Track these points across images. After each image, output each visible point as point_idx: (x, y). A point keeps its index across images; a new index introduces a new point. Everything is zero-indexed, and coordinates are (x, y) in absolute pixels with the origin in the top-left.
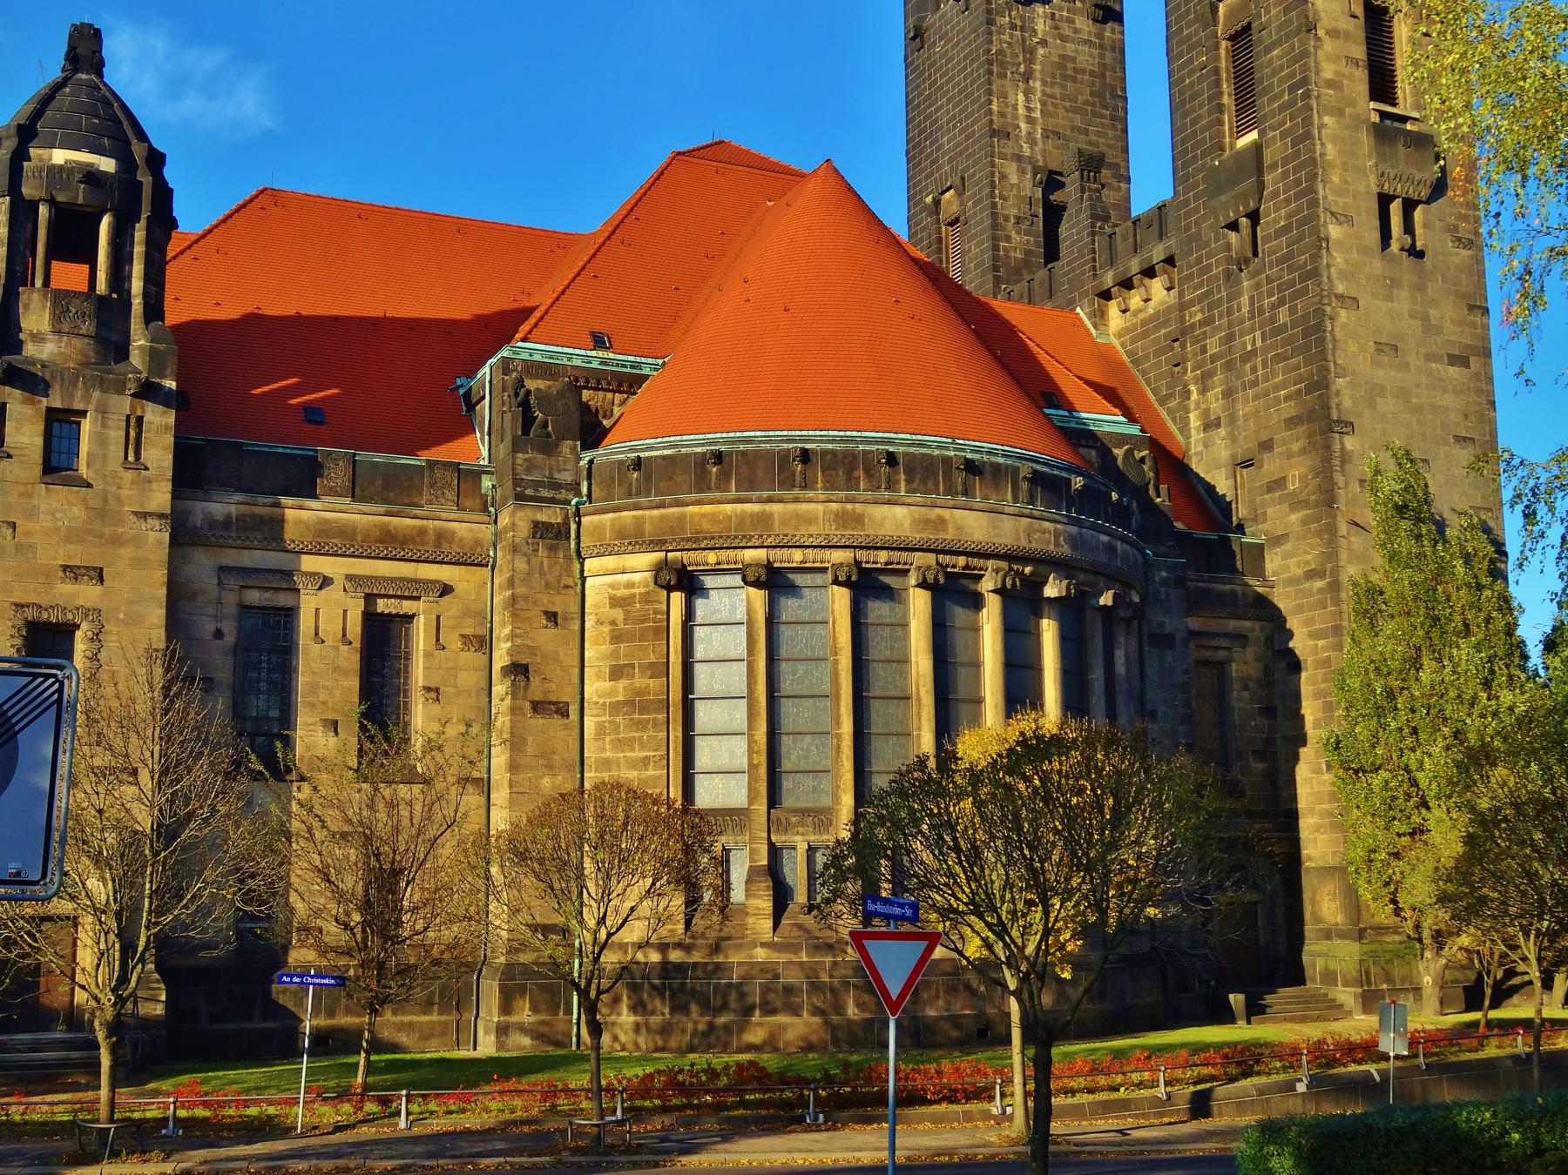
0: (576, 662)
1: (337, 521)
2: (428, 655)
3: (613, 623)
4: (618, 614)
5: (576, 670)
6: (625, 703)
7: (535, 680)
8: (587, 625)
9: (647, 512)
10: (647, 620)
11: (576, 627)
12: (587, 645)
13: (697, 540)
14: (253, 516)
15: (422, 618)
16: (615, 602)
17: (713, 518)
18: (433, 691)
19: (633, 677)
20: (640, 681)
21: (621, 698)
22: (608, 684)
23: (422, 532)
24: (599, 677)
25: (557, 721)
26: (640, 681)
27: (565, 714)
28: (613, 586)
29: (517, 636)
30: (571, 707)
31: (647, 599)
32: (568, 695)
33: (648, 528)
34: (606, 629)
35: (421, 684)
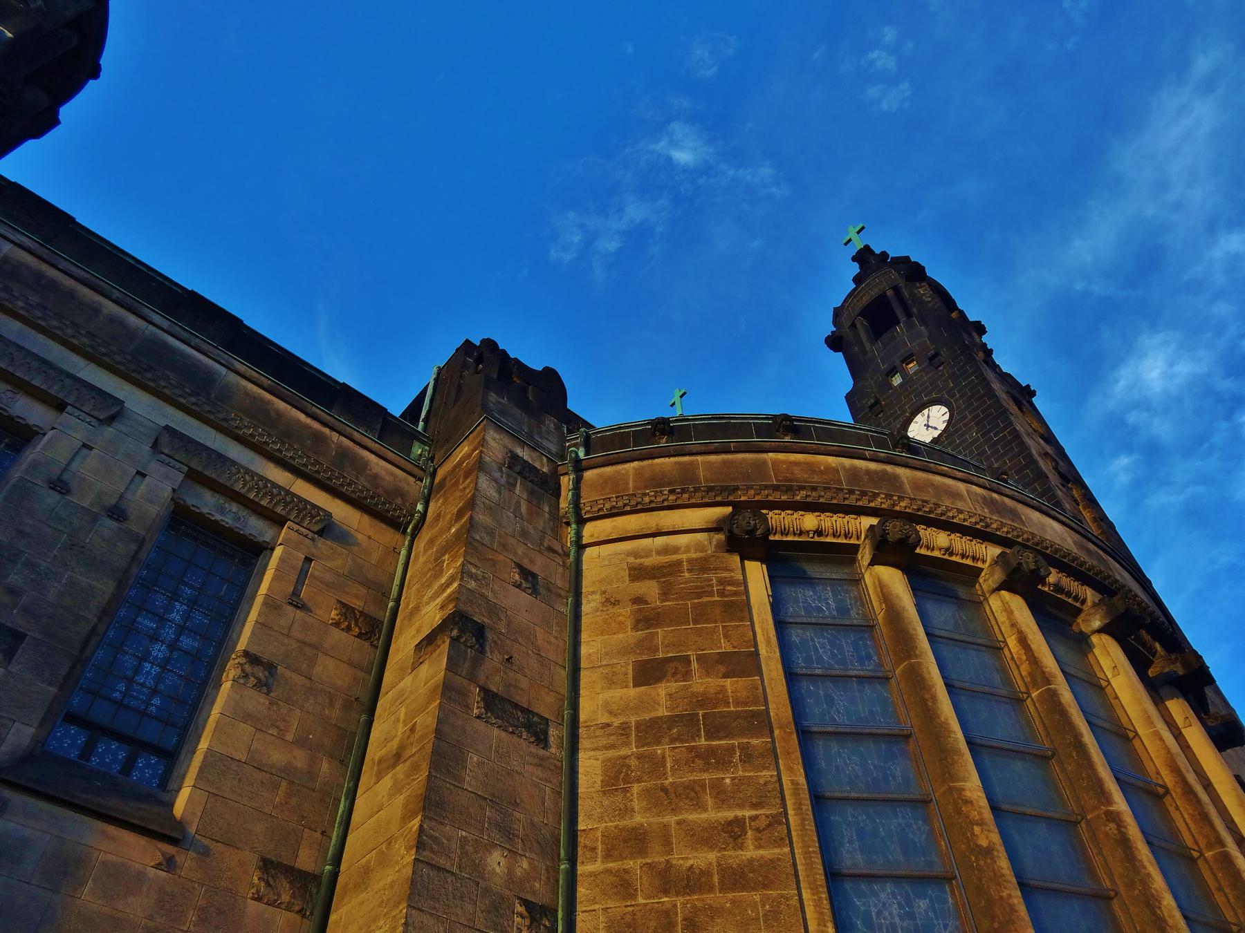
0: (566, 659)
1: (188, 356)
2: (270, 604)
3: (638, 600)
4: (650, 589)
5: (563, 675)
6: (673, 720)
7: (493, 659)
8: (586, 608)
9: (699, 458)
10: (711, 594)
11: (567, 610)
12: (584, 636)
13: (789, 489)
14: (39, 276)
15: (278, 551)
16: (638, 573)
17: (811, 467)
18: (262, 670)
19: (687, 676)
20: (701, 683)
21: (662, 712)
22: (633, 692)
23: (319, 439)
24: (611, 681)
25: (523, 744)
26: (701, 683)
27: (541, 739)
28: (636, 554)
29: (471, 576)
30: (553, 732)
31: (701, 566)
32: (545, 705)
33: (701, 473)
34: (626, 612)
35: (241, 645)
